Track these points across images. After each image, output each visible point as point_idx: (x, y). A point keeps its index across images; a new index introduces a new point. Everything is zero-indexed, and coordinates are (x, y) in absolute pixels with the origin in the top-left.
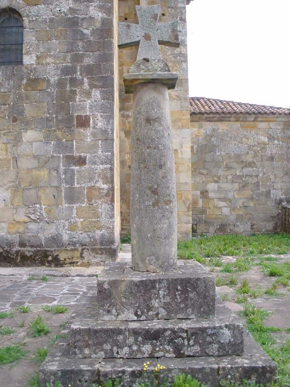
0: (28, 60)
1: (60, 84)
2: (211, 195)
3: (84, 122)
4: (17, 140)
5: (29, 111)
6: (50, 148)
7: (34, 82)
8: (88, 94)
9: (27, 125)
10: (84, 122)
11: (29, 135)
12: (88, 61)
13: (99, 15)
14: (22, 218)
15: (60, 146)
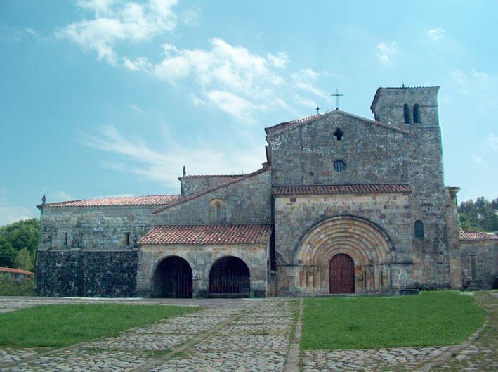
0: (425, 235)
1: (434, 243)
2: (466, 274)
3: (441, 253)
4: (424, 258)
5: (427, 250)
6: (433, 260)
7: (427, 242)
8: (442, 245)
9: (426, 253)
10: (441, 253)
11: (427, 256)
12: (441, 236)
13: (444, 223)
14: (426, 278)
15: (435, 259)
